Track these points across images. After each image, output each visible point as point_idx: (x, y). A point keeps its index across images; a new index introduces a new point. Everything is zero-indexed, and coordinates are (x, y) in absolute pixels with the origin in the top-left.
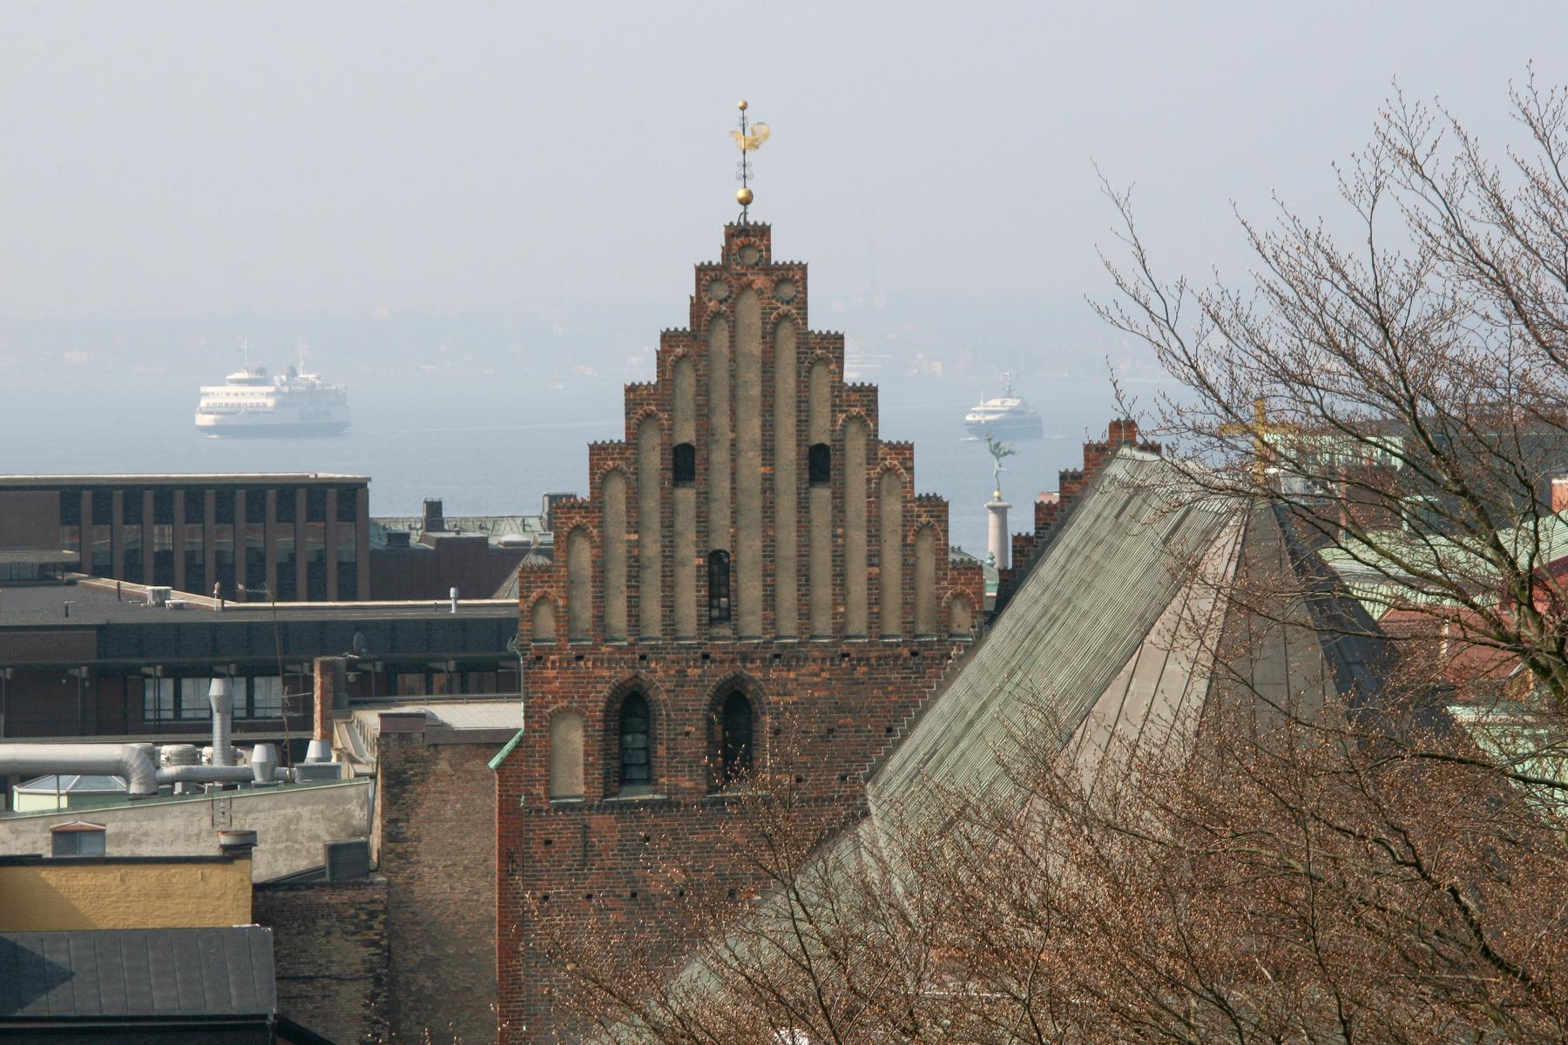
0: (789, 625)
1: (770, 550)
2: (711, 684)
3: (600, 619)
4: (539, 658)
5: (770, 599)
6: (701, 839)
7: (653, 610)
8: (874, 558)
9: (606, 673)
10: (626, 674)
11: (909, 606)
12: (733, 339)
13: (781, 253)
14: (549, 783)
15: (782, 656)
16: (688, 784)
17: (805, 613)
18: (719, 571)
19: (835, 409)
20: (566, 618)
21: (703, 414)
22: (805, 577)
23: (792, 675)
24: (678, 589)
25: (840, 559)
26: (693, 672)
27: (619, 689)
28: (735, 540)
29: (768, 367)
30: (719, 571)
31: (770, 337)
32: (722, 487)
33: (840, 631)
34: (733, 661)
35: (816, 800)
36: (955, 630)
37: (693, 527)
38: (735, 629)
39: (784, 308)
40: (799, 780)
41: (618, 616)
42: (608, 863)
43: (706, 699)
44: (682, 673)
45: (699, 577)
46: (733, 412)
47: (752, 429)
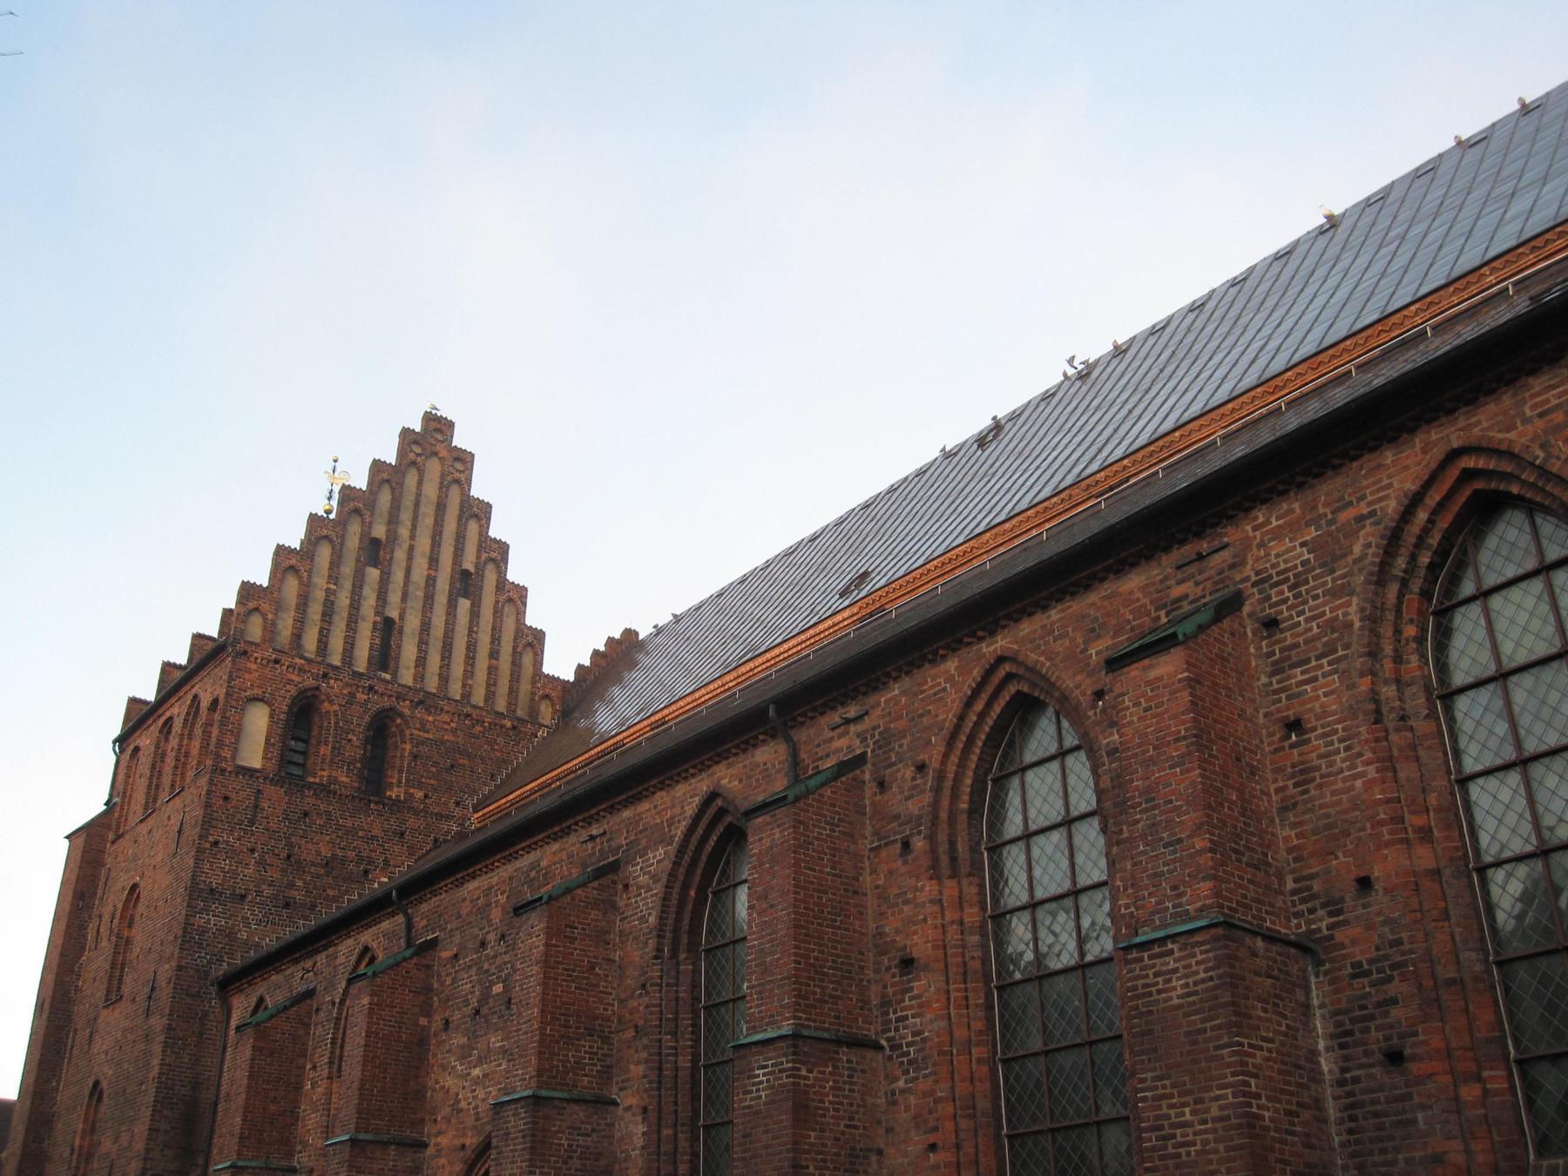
0: (432, 684)
1: (426, 627)
3: (297, 637)
4: (245, 653)
5: (421, 662)
6: (349, 824)
8: (494, 654)
9: (294, 677)
10: (311, 682)
11: (513, 691)
12: (420, 483)
13: (459, 441)
14: (234, 758)
15: (426, 701)
16: (344, 779)
17: (444, 678)
18: (388, 629)
19: (480, 548)
20: (270, 629)
21: (393, 521)
23: (431, 719)
24: (358, 636)
25: (471, 647)
26: (361, 697)
27: (302, 692)
28: (402, 617)
29: (441, 507)
30: (388, 629)
31: (443, 488)
32: (398, 576)
33: (467, 695)
34: (390, 696)
35: (436, 814)
36: (542, 721)
38: (395, 674)
39: (457, 475)
40: (426, 796)
41: (310, 643)
42: (273, 826)
43: (367, 718)
44: (352, 695)
45: (374, 630)
46: (414, 526)
47: (424, 543)
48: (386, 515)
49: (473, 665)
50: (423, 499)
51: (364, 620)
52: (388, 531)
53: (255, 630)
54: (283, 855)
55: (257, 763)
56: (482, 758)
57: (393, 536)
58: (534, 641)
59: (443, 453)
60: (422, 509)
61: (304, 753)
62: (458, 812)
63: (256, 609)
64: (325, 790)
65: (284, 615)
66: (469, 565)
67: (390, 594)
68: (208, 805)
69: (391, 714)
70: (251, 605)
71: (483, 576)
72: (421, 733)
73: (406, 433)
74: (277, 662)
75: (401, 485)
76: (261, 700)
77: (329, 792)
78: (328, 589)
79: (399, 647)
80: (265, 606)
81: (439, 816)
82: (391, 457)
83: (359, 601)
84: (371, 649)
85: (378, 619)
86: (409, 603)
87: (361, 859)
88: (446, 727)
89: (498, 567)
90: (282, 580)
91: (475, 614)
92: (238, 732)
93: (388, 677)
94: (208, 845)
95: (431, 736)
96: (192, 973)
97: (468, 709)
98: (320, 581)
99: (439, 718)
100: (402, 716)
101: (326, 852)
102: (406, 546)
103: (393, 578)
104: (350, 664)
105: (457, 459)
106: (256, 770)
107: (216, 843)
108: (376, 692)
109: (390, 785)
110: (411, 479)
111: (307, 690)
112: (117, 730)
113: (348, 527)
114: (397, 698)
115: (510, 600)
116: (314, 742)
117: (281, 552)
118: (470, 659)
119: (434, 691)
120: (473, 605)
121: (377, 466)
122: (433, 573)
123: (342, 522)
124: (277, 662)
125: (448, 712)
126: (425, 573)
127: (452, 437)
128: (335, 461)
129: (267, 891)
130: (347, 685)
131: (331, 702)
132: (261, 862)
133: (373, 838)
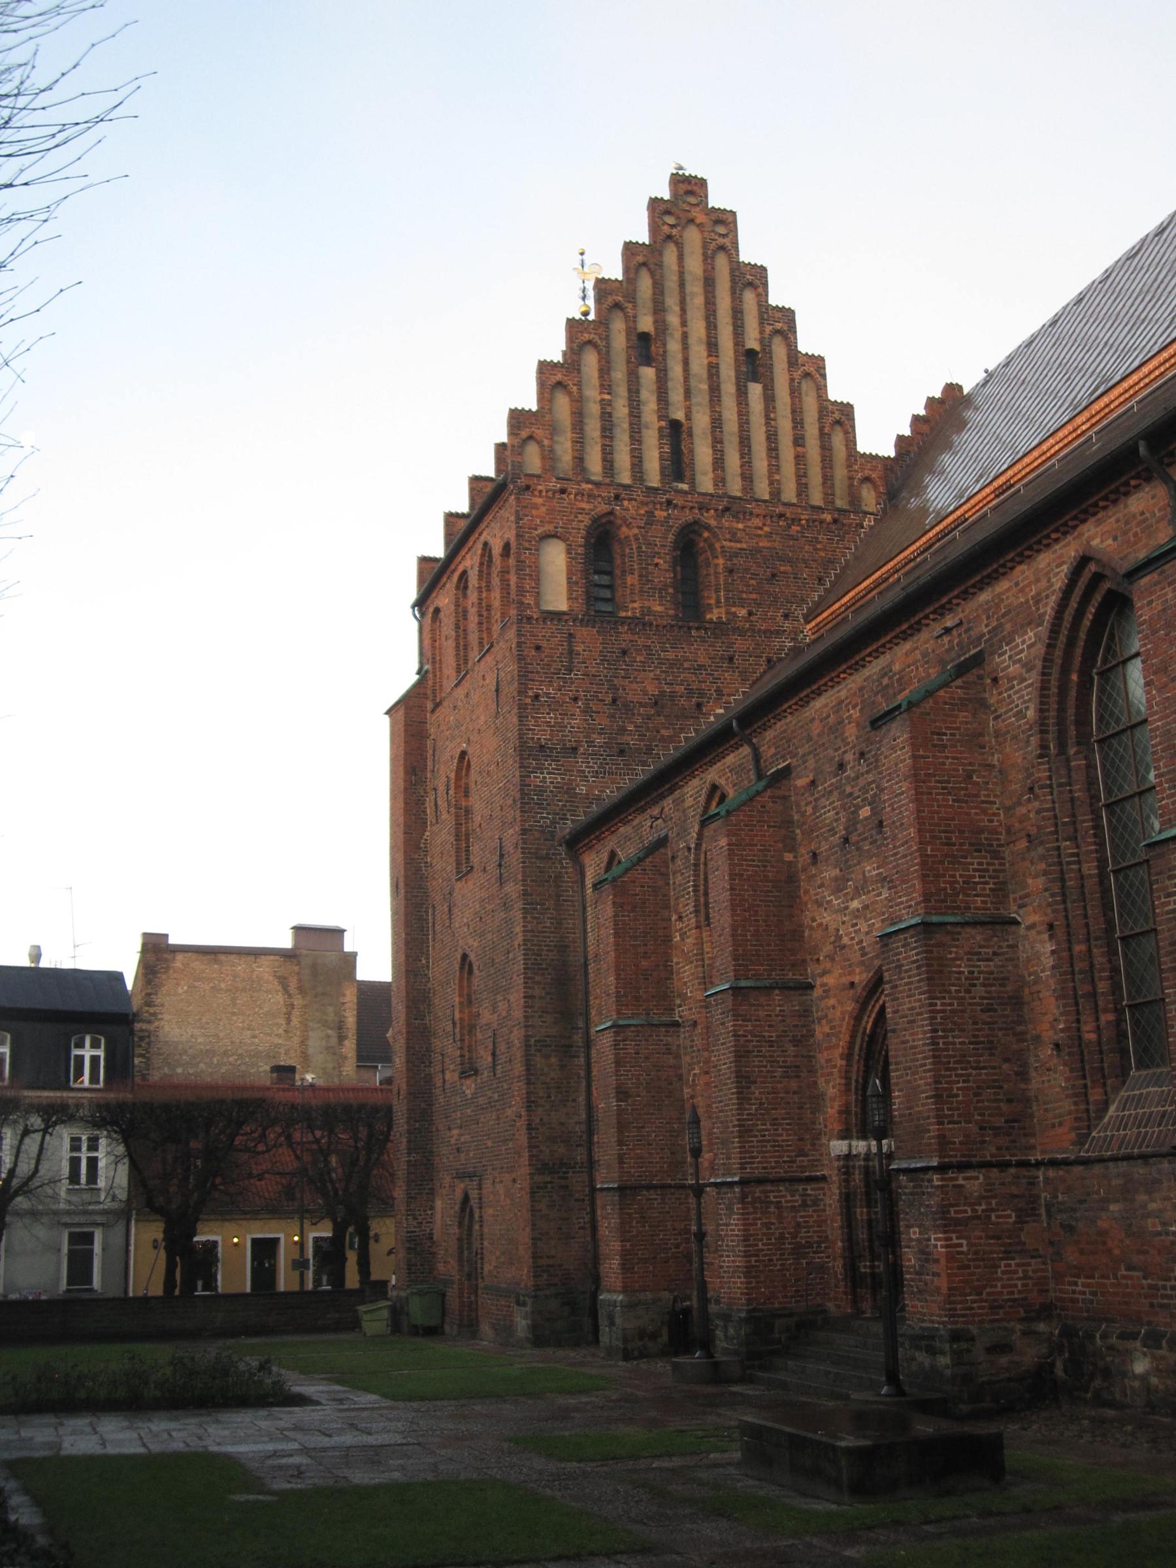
0: (735, 487)
1: (717, 423)
2: (676, 525)
3: (579, 461)
4: (528, 488)
5: (719, 463)
6: (671, 655)
7: (623, 459)
8: (799, 441)
9: (584, 505)
10: (603, 508)
11: (827, 479)
12: (681, 258)
14: (537, 604)
15: (732, 507)
16: (658, 608)
17: (747, 477)
18: (675, 432)
19: (762, 321)
20: (549, 457)
21: (659, 309)
22: (745, 442)
23: (740, 526)
24: (644, 447)
25: (772, 438)
26: (660, 514)
28: (688, 416)
29: (709, 283)
30: (675, 432)
31: (708, 259)
33: (776, 493)
34: (692, 508)
35: (765, 632)
37: (654, 398)
38: (693, 483)
39: (721, 241)
40: (750, 614)
41: (595, 464)
42: (593, 671)
43: (671, 537)
44: (650, 514)
45: (661, 437)
46: (683, 310)
47: (698, 328)
48: (650, 304)
49: (777, 458)
50: (688, 277)
51: (647, 428)
52: (655, 322)
53: (533, 460)
54: (609, 699)
55: (563, 606)
56: (805, 561)
57: (662, 326)
58: (843, 416)
59: (701, 218)
60: (689, 289)
61: (610, 587)
62: (787, 625)
63: (531, 437)
64: (640, 624)
65: (561, 439)
66: (752, 343)
67: (670, 392)
68: (521, 658)
69: (696, 527)
70: (524, 434)
71: (770, 353)
72: (732, 544)
73: (655, 204)
74: (563, 491)
75: (660, 265)
76: (555, 536)
77: (644, 624)
78: (603, 400)
79: (691, 451)
80: (539, 433)
81: (768, 633)
82: (642, 236)
83: (638, 407)
84: (661, 459)
85: (663, 423)
86: (694, 400)
87: (690, 692)
88: (760, 532)
89: (786, 338)
90: (551, 401)
91: (769, 398)
92: (536, 576)
93: (685, 487)
94: (529, 701)
95: (744, 546)
96: (537, 835)
97: (780, 509)
98: (592, 393)
99: (749, 524)
100: (708, 528)
101: (652, 690)
102: (678, 335)
103: (671, 374)
104: (642, 480)
105: (718, 222)
106: (564, 613)
107: (537, 697)
108: (676, 506)
109: (709, 608)
110: (670, 256)
111: (600, 517)
112: (412, 594)
113: (610, 326)
114: (700, 509)
115: (807, 375)
116: (618, 572)
117: (545, 368)
118: (773, 450)
119: (739, 494)
120: (765, 388)
121: (630, 249)
122: (713, 360)
123: (603, 321)
124: (563, 491)
125: (758, 516)
126: (706, 362)
127: (706, 197)
128: (582, 254)
129: (599, 740)
130: (644, 504)
131: (629, 526)
132: (586, 711)
133: (701, 667)
